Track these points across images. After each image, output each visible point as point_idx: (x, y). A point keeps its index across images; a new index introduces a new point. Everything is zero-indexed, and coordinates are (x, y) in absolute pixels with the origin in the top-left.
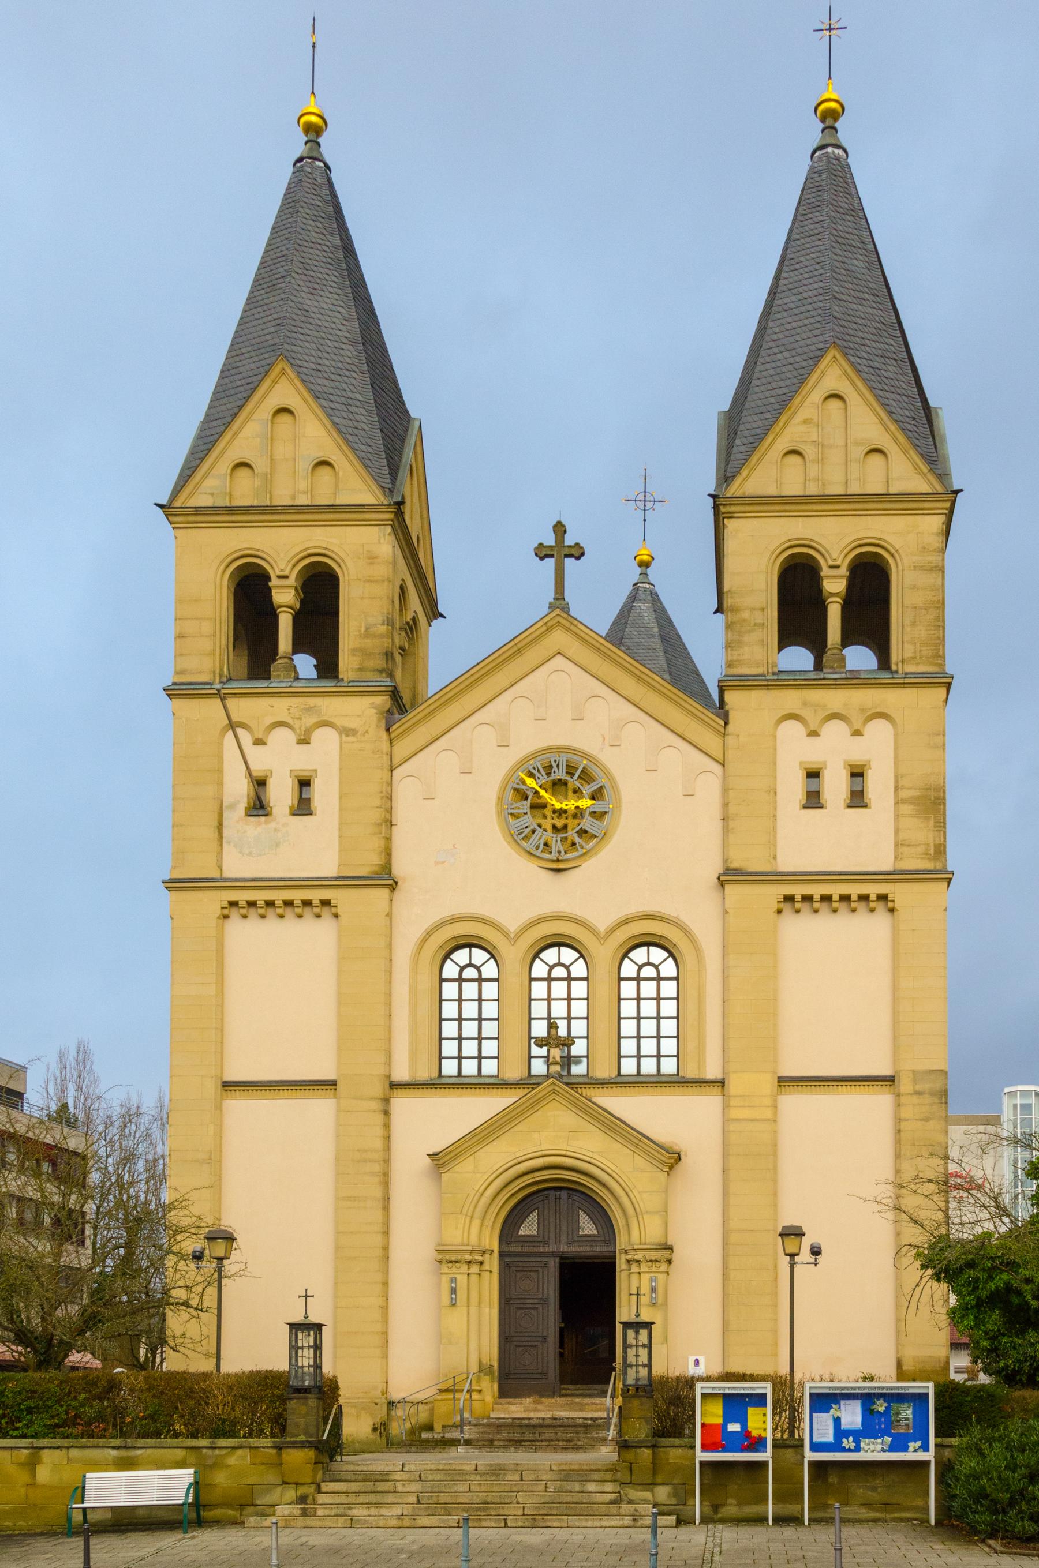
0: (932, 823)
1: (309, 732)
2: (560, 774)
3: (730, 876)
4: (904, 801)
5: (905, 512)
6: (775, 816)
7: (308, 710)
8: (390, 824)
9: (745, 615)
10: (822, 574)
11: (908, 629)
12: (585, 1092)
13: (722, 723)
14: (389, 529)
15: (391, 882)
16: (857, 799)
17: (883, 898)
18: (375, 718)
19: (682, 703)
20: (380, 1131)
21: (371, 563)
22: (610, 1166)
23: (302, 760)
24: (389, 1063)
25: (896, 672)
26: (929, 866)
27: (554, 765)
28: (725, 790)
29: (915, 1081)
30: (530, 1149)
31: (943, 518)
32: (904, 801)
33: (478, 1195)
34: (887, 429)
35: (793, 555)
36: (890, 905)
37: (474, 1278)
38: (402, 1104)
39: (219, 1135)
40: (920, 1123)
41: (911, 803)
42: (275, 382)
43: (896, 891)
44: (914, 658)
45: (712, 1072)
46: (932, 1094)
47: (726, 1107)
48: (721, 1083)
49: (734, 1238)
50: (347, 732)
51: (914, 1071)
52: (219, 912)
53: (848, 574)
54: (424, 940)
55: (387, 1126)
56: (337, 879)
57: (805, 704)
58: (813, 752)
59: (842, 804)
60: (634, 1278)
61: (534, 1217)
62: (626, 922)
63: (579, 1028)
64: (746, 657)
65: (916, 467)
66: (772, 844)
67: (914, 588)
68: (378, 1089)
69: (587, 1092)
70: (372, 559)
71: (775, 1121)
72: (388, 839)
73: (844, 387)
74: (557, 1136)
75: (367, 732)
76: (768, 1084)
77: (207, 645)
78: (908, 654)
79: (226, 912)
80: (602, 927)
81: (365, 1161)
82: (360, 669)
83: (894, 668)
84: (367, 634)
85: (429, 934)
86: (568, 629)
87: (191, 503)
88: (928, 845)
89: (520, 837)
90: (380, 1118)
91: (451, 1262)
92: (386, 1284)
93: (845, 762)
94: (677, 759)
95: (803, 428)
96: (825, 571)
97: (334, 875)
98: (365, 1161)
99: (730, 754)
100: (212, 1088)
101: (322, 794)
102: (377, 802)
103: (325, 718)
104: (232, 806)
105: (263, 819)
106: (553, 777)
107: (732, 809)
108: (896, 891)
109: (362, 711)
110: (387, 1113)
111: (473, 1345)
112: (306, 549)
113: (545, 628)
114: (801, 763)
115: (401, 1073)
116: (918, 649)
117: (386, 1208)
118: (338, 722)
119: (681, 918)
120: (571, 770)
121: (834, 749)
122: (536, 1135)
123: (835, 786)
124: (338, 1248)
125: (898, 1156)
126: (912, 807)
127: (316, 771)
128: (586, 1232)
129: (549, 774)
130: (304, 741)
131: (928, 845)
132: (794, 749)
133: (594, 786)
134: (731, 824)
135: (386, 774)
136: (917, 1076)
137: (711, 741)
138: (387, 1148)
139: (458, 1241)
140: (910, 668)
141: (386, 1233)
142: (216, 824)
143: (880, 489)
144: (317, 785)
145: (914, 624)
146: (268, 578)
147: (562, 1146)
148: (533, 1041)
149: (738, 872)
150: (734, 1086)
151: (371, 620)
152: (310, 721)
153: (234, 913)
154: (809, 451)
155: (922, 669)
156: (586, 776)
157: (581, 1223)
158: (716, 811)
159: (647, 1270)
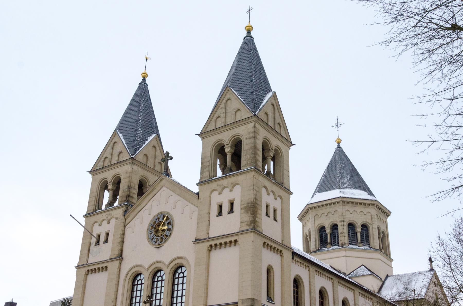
5: (245, 124)
8: (123, 242)
16: (231, 210)
26: (248, 228)
43: (240, 239)
50: (117, 218)
51: (242, 300)
56: (110, 259)
57: (218, 185)
62: (173, 261)
67: (247, 144)
95: (221, 110)
102: (120, 236)
123: (226, 208)
133: (169, 221)
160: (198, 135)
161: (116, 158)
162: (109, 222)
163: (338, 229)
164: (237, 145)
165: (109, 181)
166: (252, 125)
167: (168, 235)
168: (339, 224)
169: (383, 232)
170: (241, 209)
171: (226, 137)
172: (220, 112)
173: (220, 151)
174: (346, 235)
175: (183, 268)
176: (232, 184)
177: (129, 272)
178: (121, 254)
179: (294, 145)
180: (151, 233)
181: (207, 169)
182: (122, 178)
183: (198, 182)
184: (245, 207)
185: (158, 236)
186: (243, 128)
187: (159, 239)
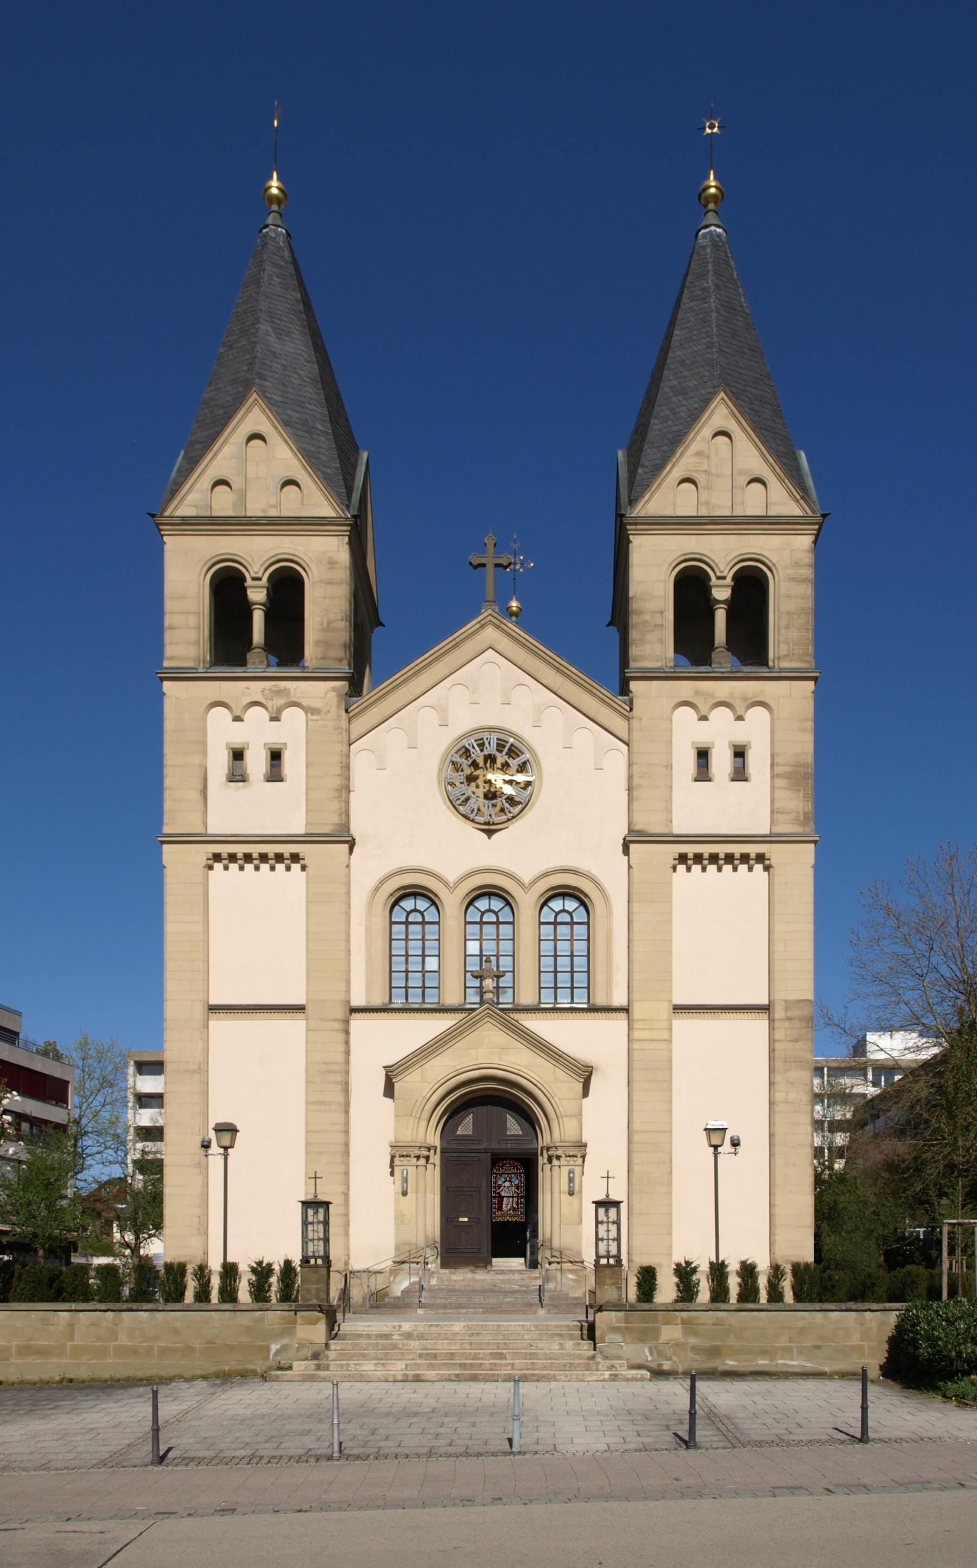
0: (801, 794)
1: (280, 710)
2: (491, 749)
4: (779, 776)
6: (671, 787)
7: (279, 692)
9: (647, 617)
10: (711, 584)
11: (783, 631)
12: (512, 1015)
13: (628, 709)
14: (346, 539)
15: (350, 839)
16: (740, 774)
17: (761, 858)
18: (335, 700)
19: (594, 691)
20: (342, 1048)
21: (331, 568)
22: (535, 1077)
23: (274, 734)
24: (348, 991)
25: (774, 667)
26: (799, 829)
27: (486, 743)
28: (630, 765)
29: (787, 1009)
30: (467, 1062)
31: (812, 538)
32: (779, 776)
33: (425, 1101)
34: (766, 460)
36: (767, 862)
37: (421, 1169)
38: (358, 1024)
39: (207, 1051)
40: (790, 1045)
41: (786, 778)
42: (249, 411)
43: (774, 852)
44: (788, 655)
45: (619, 999)
46: (801, 1019)
47: (630, 1028)
48: (626, 1010)
49: (636, 1137)
51: (786, 1001)
52: (204, 862)
53: (732, 584)
54: (377, 889)
55: (347, 1043)
57: (697, 693)
58: (703, 733)
59: (727, 778)
60: (556, 1169)
61: (469, 1120)
62: (546, 874)
63: (506, 963)
64: (647, 653)
65: (791, 494)
66: (669, 810)
67: (788, 596)
68: (340, 1012)
69: (515, 1016)
70: (332, 563)
71: (671, 1041)
72: (348, 802)
73: (732, 425)
74: (490, 1051)
75: (329, 711)
76: (664, 1010)
77: (192, 635)
79: (210, 862)
80: (526, 879)
81: (330, 1072)
82: (323, 658)
83: (771, 664)
84: (328, 628)
85: (382, 882)
86: (498, 627)
87: (179, 513)
88: (799, 813)
89: (458, 804)
90: (341, 1036)
91: (403, 1156)
92: (347, 1174)
93: (730, 743)
94: (589, 735)
95: (696, 459)
96: (714, 581)
97: (302, 831)
98: (330, 1072)
99: (636, 735)
100: (199, 1010)
101: (293, 764)
102: (338, 771)
103: (294, 699)
105: (241, 784)
106: (486, 752)
107: (636, 781)
108: (774, 852)
109: (324, 693)
110: (347, 1032)
111: (421, 1224)
112: (276, 555)
113: (478, 626)
114: (693, 743)
115: (358, 1000)
116: (791, 648)
117: (347, 1112)
118: (305, 703)
119: (593, 872)
120: (500, 747)
121: (720, 732)
122: (473, 1051)
123: (721, 762)
124: (307, 1144)
125: (771, 1071)
126: (785, 781)
127: (285, 744)
128: (513, 1133)
129: (482, 750)
130: (275, 719)
132: (687, 731)
134: (635, 793)
135: (345, 746)
136: (788, 1004)
137: (618, 724)
138: (347, 1062)
139: (408, 1138)
140: (785, 664)
141: (347, 1132)
142: (202, 788)
143: (761, 512)
144: (287, 757)
146: (244, 580)
147: (495, 1060)
148: (468, 975)
149: (641, 833)
150: (637, 1012)
151: (331, 616)
152: (280, 702)
153: (218, 866)
155: (795, 665)
156: (513, 752)
157: (509, 1125)
158: (623, 784)
159: (565, 1163)
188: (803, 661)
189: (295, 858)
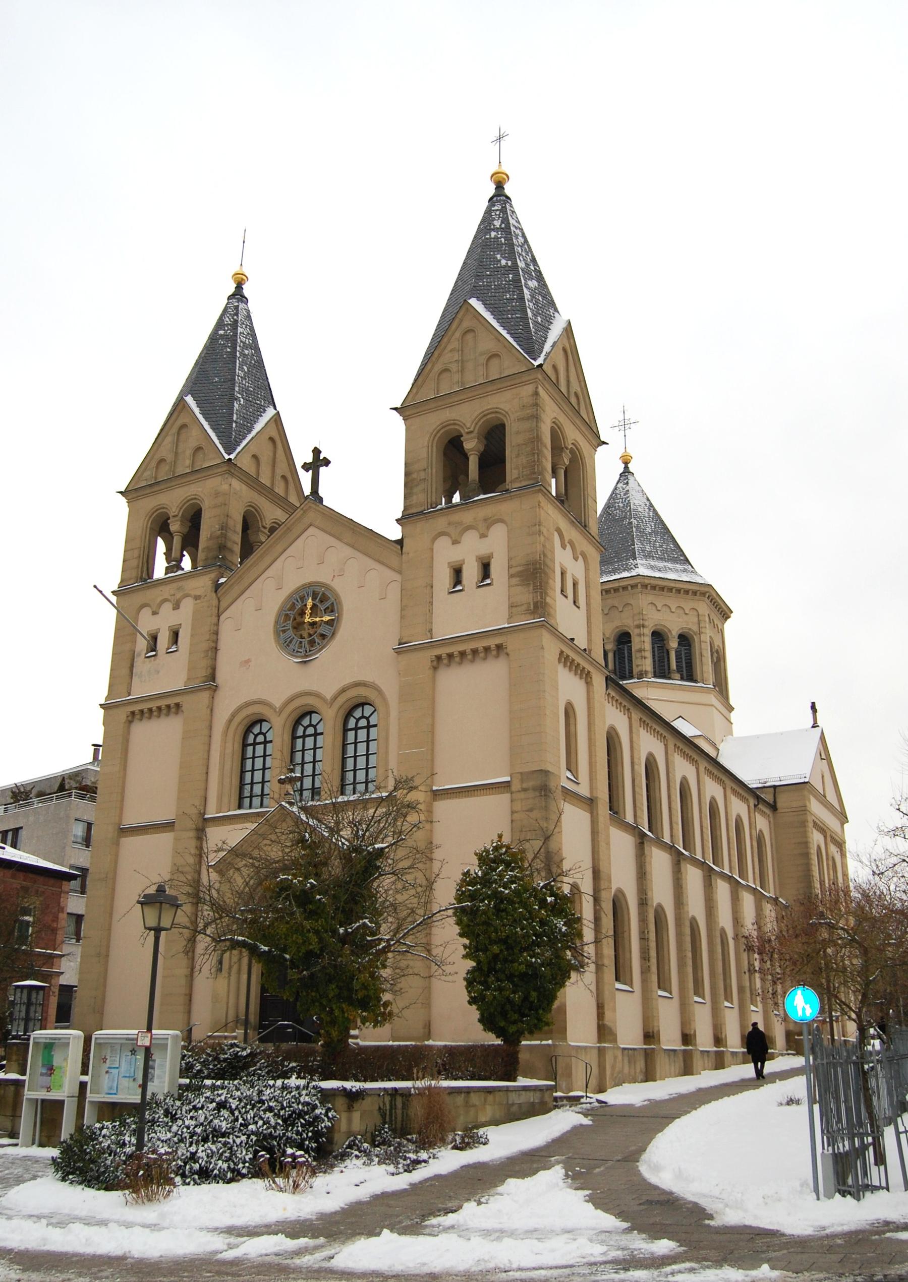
3: (403, 648)
8: (216, 649)
17: (499, 647)
29: (522, 781)
35: (446, 432)
46: (534, 789)
50: (197, 598)
57: (449, 524)
62: (343, 690)
67: (518, 433)
78: (515, 476)
79: (130, 718)
84: (211, 538)
88: (529, 604)
95: (450, 355)
104: (139, 655)
121: (468, 549)
123: (471, 573)
126: (518, 579)
131: (529, 604)
133: (328, 604)
142: (129, 665)
145: (518, 456)
154: (454, 367)
160: (395, 409)
161: (188, 462)
162: (176, 607)
163: (630, 642)
164: (494, 435)
165: (171, 515)
166: (530, 389)
167: (329, 634)
168: (634, 632)
169: (717, 652)
170: (511, 576)
171: (468, 417)
172: (448, 357)
173: (452, 447)
174: (648, 654)
175: (264, 724)
176: (485, 520)
177: (233, 715)
178: (213, 677)
179: (604, 443)
180: (284, 631)
181: (422, 486)
182: (205, 506)
183: (399, 516)
184: (521, 572)
185: (302, 637)
186: (508, 395)
187: (305, 642)
188: (530, 479)
189: (178, 705)
